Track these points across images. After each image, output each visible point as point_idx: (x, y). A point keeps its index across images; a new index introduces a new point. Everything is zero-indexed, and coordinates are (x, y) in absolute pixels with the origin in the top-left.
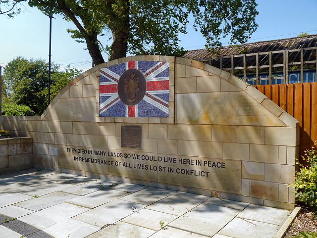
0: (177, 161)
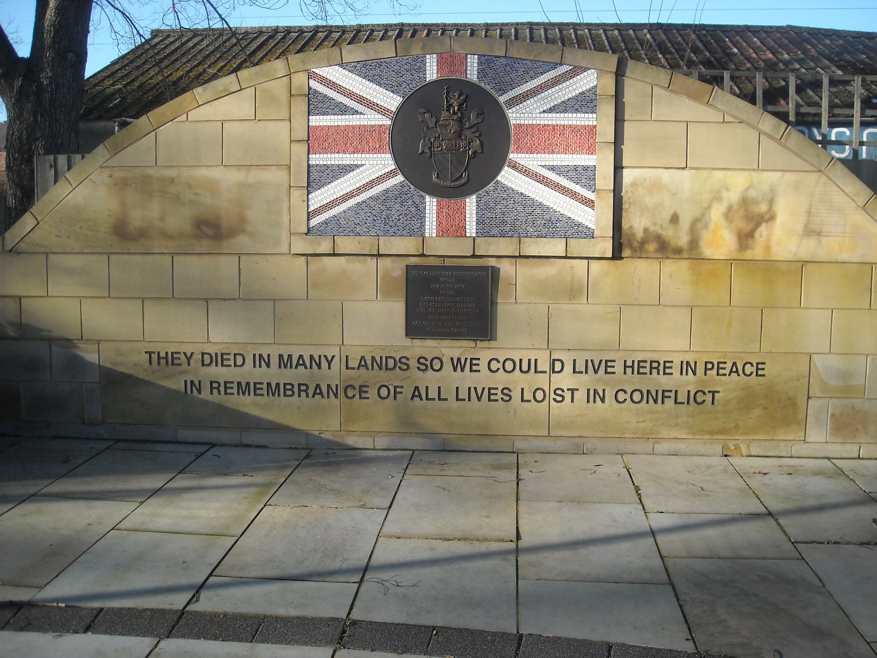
0: (619, 368)
